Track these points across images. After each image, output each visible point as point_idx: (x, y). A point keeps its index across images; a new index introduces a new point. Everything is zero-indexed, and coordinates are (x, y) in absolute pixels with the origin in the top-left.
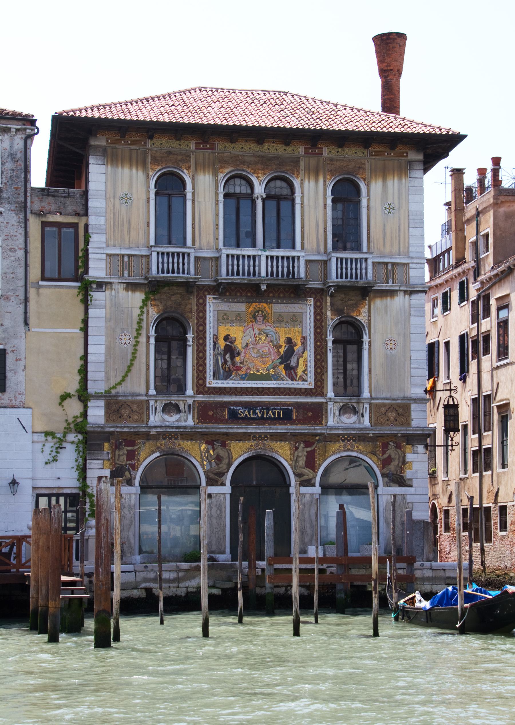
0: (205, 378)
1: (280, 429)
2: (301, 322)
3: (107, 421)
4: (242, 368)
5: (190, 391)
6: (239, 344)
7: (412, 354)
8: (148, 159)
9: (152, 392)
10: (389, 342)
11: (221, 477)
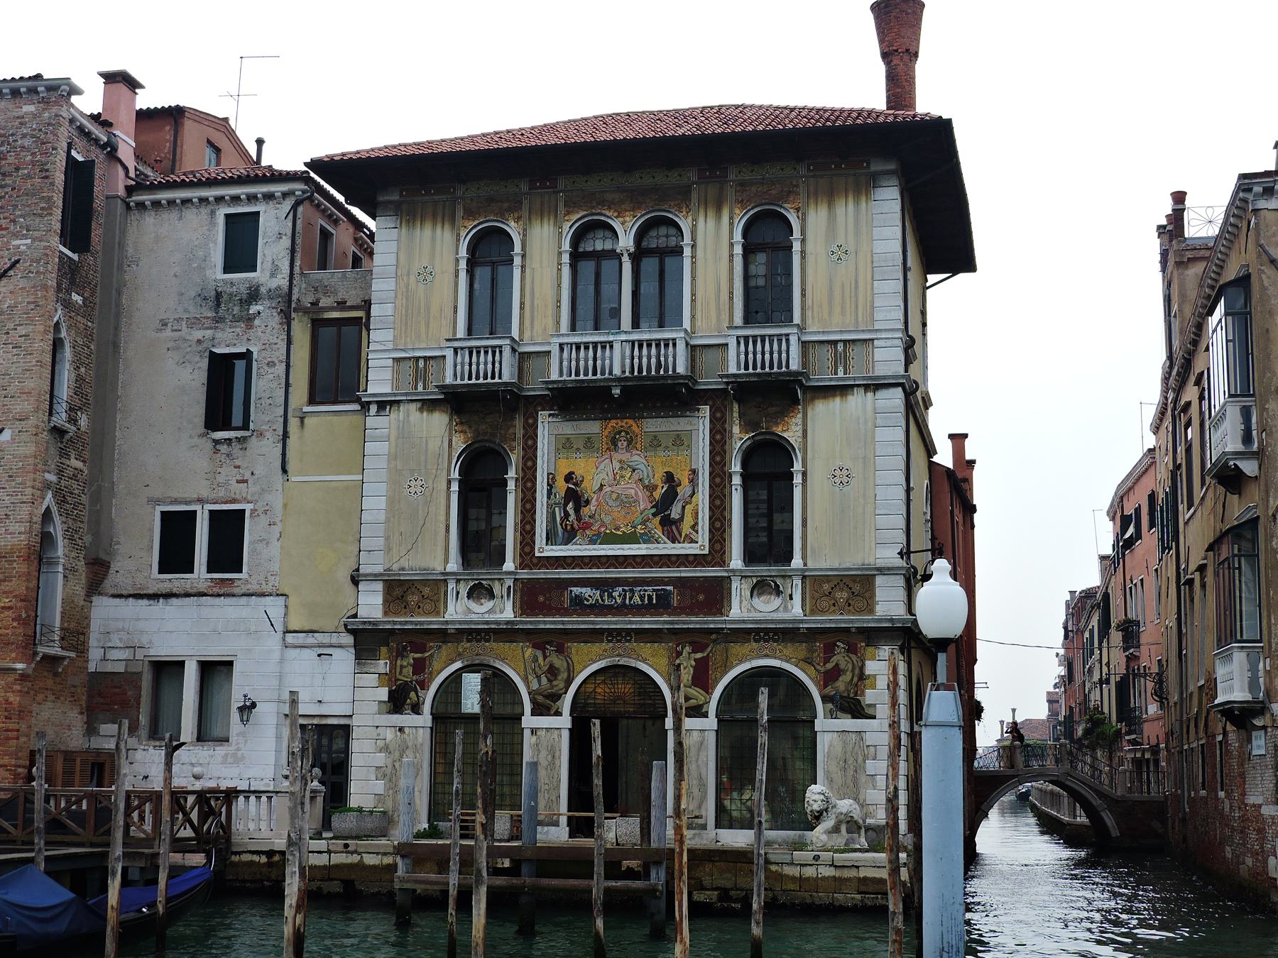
3: (386, 613)
5: (509, 565)
6: (589, 487)
7: (879, 491)
9: (454, 565)
10: (838, 473)
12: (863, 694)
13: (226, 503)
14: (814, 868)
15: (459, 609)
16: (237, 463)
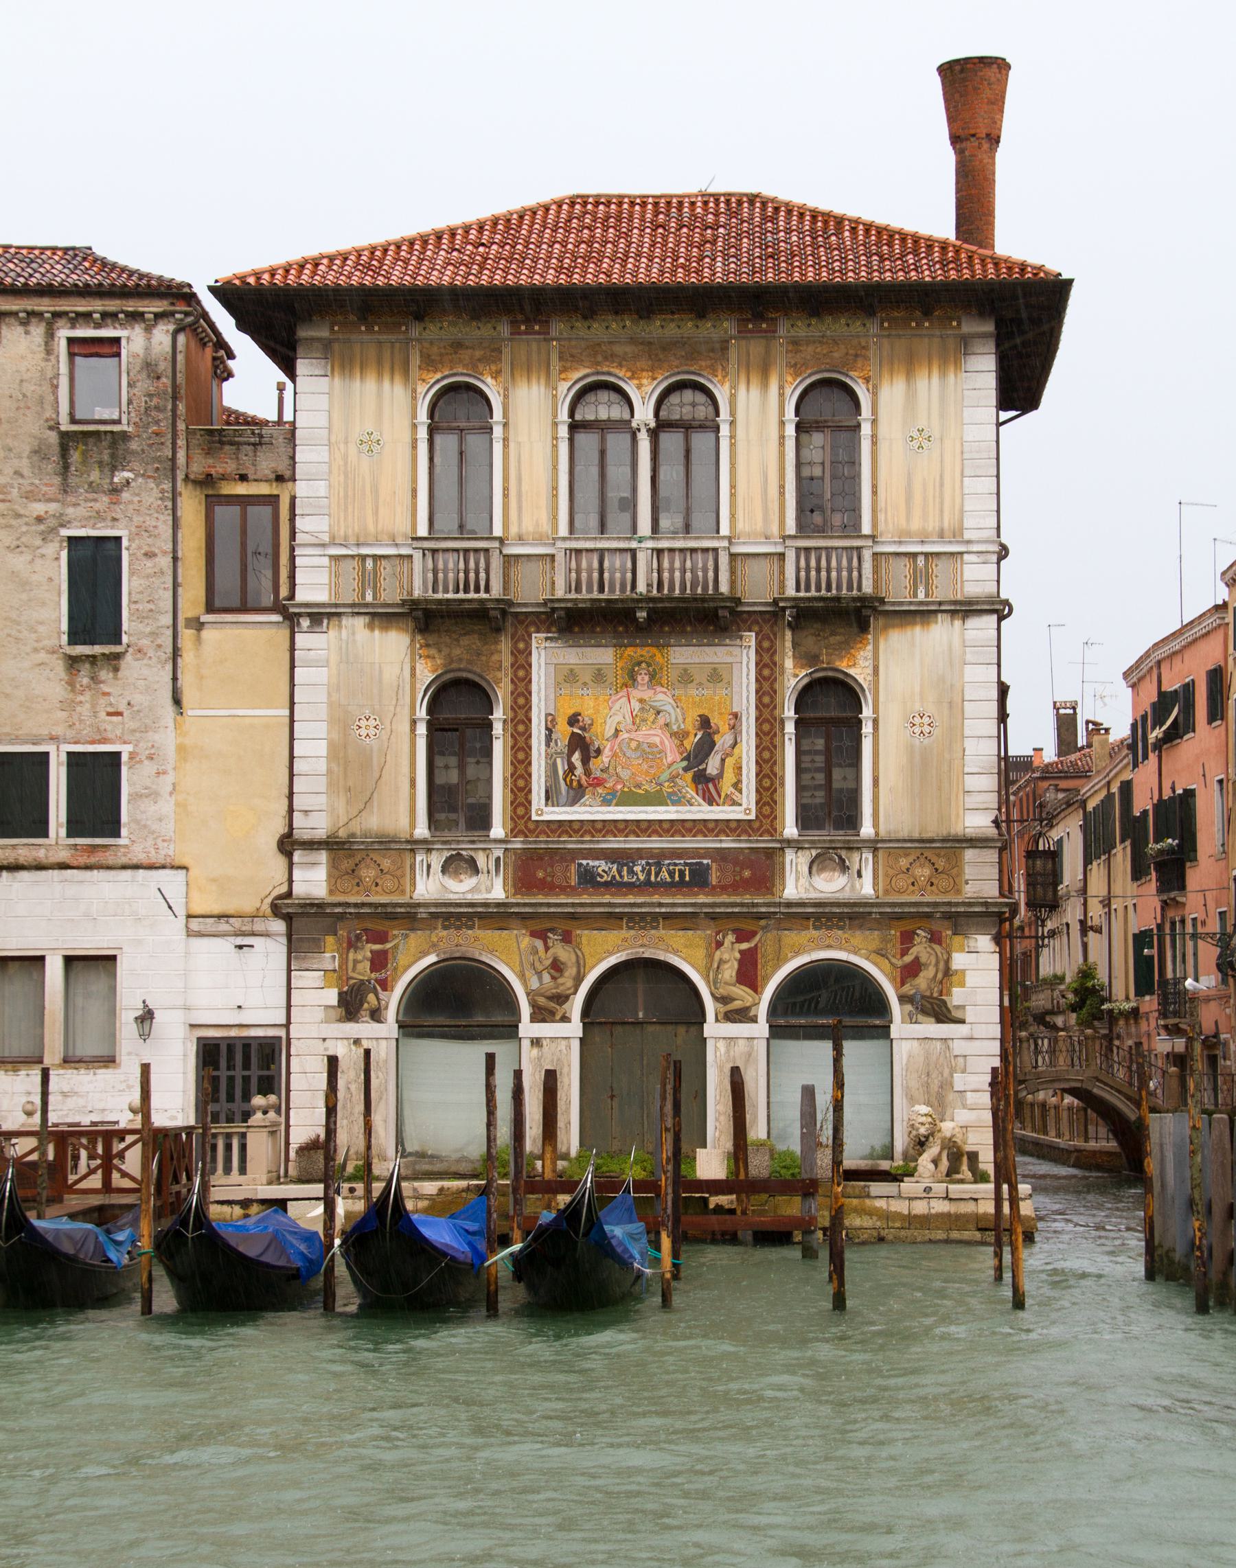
0: (530, 803)
1: (681, 901)
2: (729, 683)
3: (331, 892)
4: (605, 780)
5: (497, 831)
8: (415, 360)
10: (917, 720)
11: (561, 1004)
12: (949, 994)
13: (93, 742)
14: (925, 1202)
15: (431, 885)
16: (105, 689)
